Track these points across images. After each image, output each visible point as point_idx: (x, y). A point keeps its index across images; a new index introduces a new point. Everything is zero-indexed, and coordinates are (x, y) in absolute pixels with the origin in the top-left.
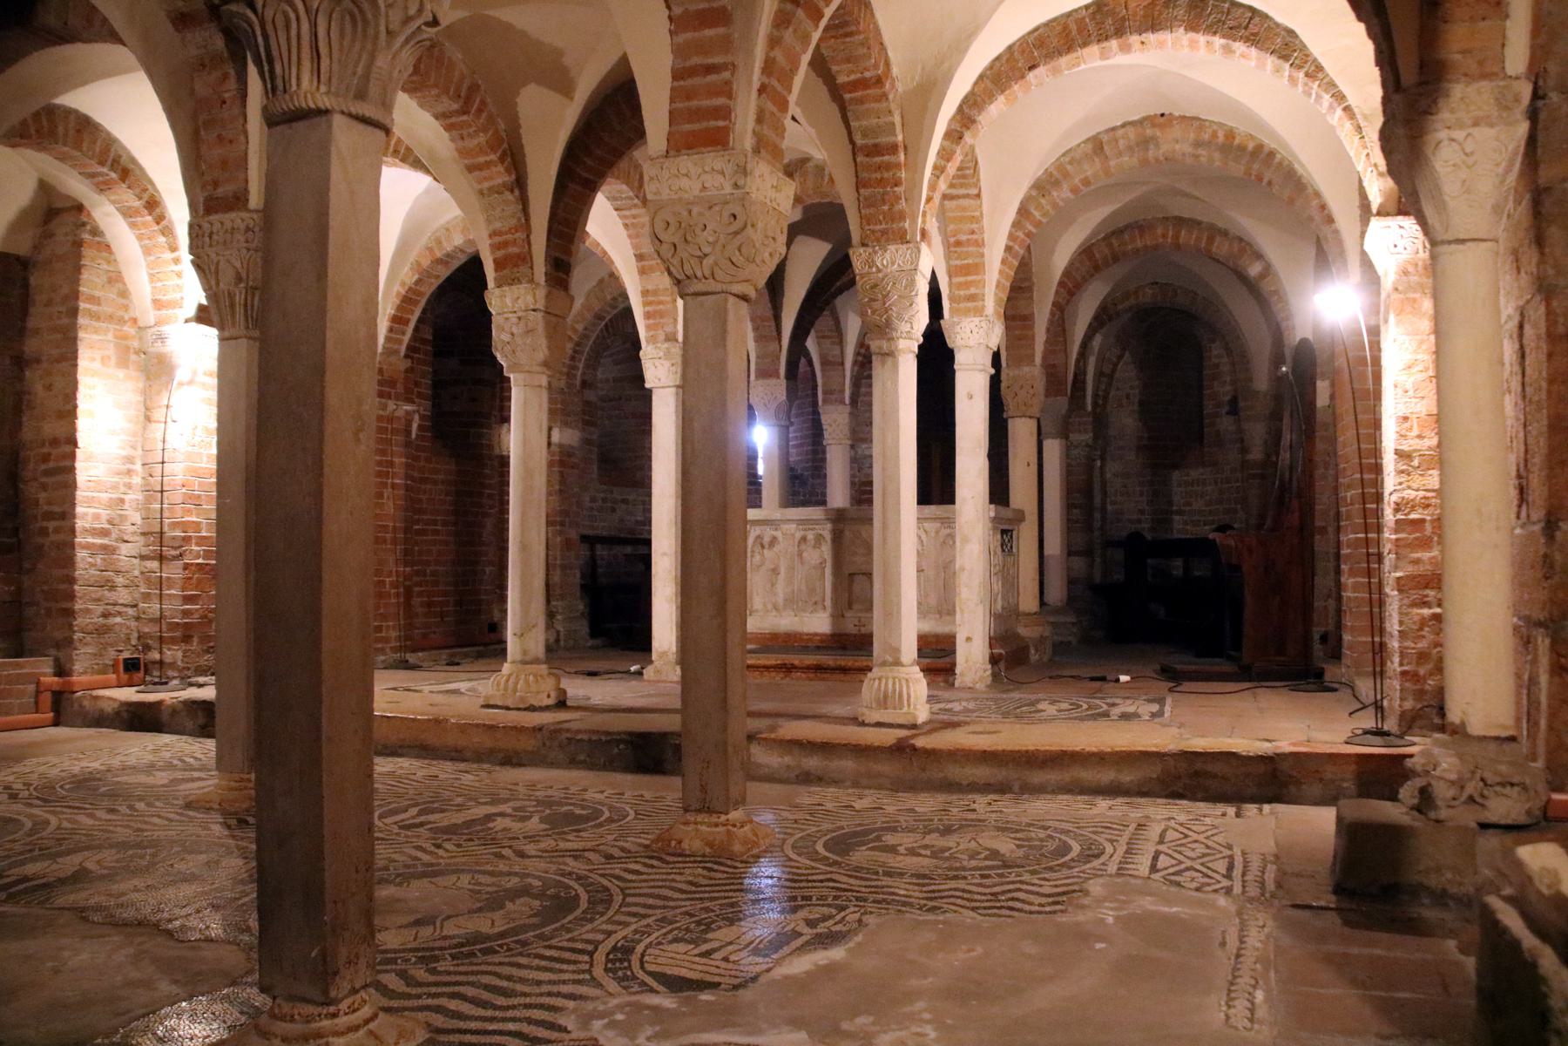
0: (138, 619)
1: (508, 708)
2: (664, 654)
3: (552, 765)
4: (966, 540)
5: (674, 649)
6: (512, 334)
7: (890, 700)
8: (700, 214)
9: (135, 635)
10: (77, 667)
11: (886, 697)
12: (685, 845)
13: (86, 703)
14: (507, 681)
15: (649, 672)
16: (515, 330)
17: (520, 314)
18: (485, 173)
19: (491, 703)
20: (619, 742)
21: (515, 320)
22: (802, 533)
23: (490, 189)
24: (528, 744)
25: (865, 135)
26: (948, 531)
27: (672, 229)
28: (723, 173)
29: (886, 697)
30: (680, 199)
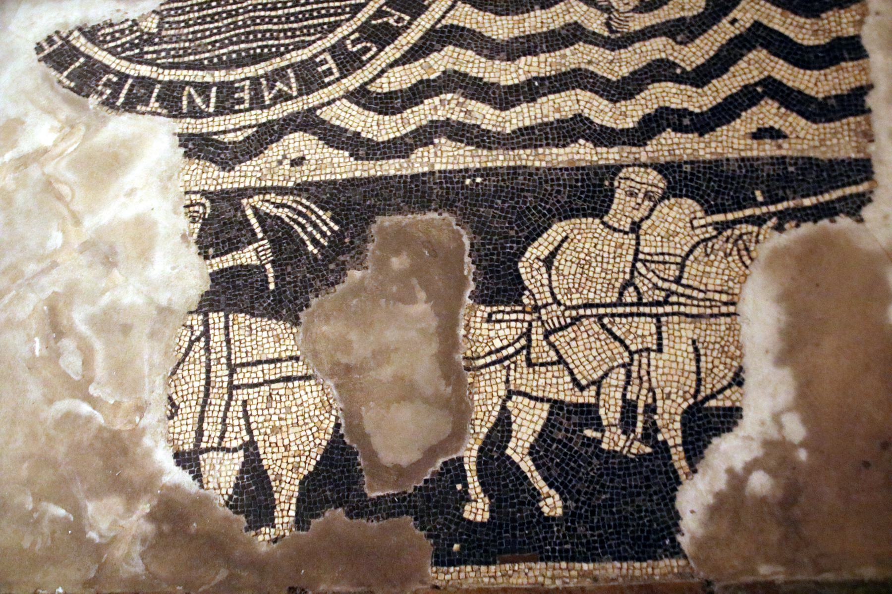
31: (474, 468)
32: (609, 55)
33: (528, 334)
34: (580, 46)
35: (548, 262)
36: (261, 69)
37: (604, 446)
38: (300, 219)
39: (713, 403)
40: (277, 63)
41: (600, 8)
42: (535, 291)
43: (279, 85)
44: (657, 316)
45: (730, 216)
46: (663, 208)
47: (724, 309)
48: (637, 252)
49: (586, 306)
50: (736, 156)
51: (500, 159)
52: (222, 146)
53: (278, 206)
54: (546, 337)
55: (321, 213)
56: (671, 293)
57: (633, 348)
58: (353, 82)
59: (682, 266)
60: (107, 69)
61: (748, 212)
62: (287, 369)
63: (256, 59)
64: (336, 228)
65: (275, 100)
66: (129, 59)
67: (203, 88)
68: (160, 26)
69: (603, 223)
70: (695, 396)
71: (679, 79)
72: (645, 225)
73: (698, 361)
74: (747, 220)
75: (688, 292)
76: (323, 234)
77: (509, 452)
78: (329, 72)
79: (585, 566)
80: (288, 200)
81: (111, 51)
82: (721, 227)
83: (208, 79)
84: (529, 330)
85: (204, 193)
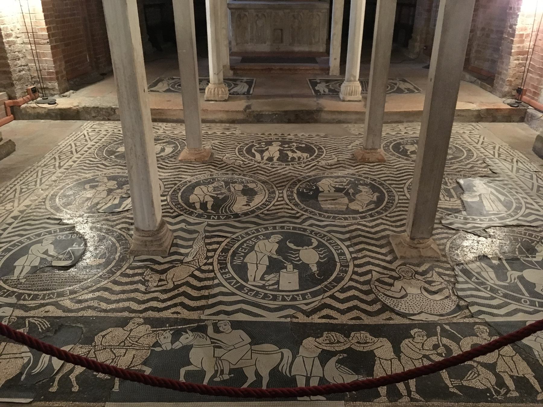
0: (29, 70)
1: (216, 101)
3: (251, 122)
4: (336, 23)
5: (229, 64)
7: (353, 93)
9: (30, 77)
10: (17, 95)
11: (352, 92)
12: (370, 160)
13: (28, 110)
14: (214, 91)
19: (209, 99)
20: (276, 114)
24: (240, 117)
29: (352, 92)
31: (58, 379)
32: (143, 295)
33: (89, 351)
34: (136, 293)
35: (103, 336)
36: (48, 292)
37: (98, 376)
38: (41, 324)
39: (133, 368)
40: (54, 291)
41: (146, 286)
42: (97, 342)
43: (51, 296)
44: (127, 349)
45: (158, 329)
46: (141, 327)
47: (146, 348)
48: (129, 335)
49: (109, 346)
50: (166, 317)
51: (103, 314)
52: (28, 307)
53: (35, 320)
54: (95, 351)
55: (47, 323)
56: (133, 344)
57: (117, 355)
58: (72, 296)
59: (139, 339)
60: (5, 289)
61: (162, 329)
62: (17, 356)
63: (49, 290)
64: (49, 326)
65: (48, 299)
66: (12, 287)
67: (29, 295)
68: (25, 281)
69: (123, 329)
70: (128, 367)
71: (158, 301)
72: (134, 330)
73: (133, 358)
74: (162, 330)
75: (138, 344)
76: (45, 327)
77: (70, 376)
78: (67, 294)
79: (77, 403)
80: (40, 320)
81: (9, 286)
82: (153, 331)
83: (32, 293)
84: (90, 351)
85: (16, 316)
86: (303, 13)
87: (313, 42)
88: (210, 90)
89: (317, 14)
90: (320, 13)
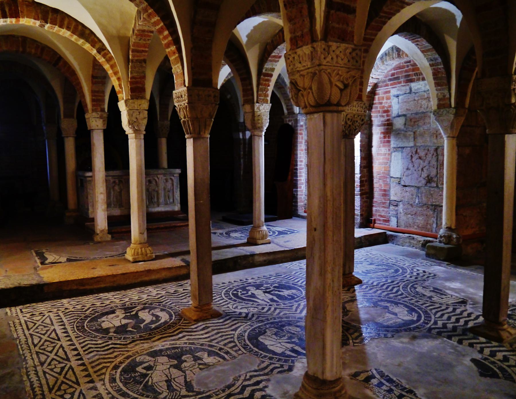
1: (144, 261)
2: (102, 231)
5: (107, 228)
6: (136, 118)
8: (356, 118)
11: (263, 235)
14: (142, 251)
15: (97, 238)
16: (138, 117)
17: (139, 111)
18: (138, 54)
19: (137, 260)
21: (138, 113)
22: (114, 180)
23: (137, 60)
25: (266, 70)
26: (165, 178)
27: (350, 120)
28: (362, 107)
30: (352, 113)
86: (158, 178)
87: (169, 202)
88: (136, 250)
89: (171, 178)
90: (173, 178)
